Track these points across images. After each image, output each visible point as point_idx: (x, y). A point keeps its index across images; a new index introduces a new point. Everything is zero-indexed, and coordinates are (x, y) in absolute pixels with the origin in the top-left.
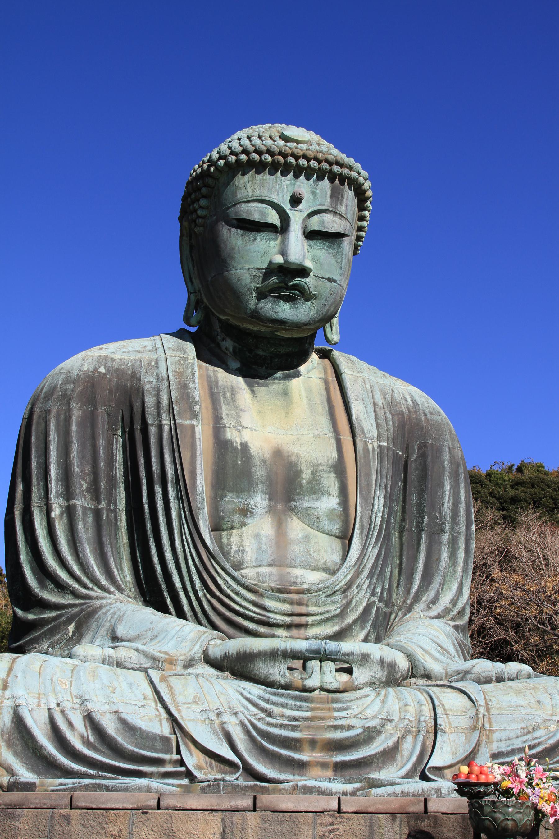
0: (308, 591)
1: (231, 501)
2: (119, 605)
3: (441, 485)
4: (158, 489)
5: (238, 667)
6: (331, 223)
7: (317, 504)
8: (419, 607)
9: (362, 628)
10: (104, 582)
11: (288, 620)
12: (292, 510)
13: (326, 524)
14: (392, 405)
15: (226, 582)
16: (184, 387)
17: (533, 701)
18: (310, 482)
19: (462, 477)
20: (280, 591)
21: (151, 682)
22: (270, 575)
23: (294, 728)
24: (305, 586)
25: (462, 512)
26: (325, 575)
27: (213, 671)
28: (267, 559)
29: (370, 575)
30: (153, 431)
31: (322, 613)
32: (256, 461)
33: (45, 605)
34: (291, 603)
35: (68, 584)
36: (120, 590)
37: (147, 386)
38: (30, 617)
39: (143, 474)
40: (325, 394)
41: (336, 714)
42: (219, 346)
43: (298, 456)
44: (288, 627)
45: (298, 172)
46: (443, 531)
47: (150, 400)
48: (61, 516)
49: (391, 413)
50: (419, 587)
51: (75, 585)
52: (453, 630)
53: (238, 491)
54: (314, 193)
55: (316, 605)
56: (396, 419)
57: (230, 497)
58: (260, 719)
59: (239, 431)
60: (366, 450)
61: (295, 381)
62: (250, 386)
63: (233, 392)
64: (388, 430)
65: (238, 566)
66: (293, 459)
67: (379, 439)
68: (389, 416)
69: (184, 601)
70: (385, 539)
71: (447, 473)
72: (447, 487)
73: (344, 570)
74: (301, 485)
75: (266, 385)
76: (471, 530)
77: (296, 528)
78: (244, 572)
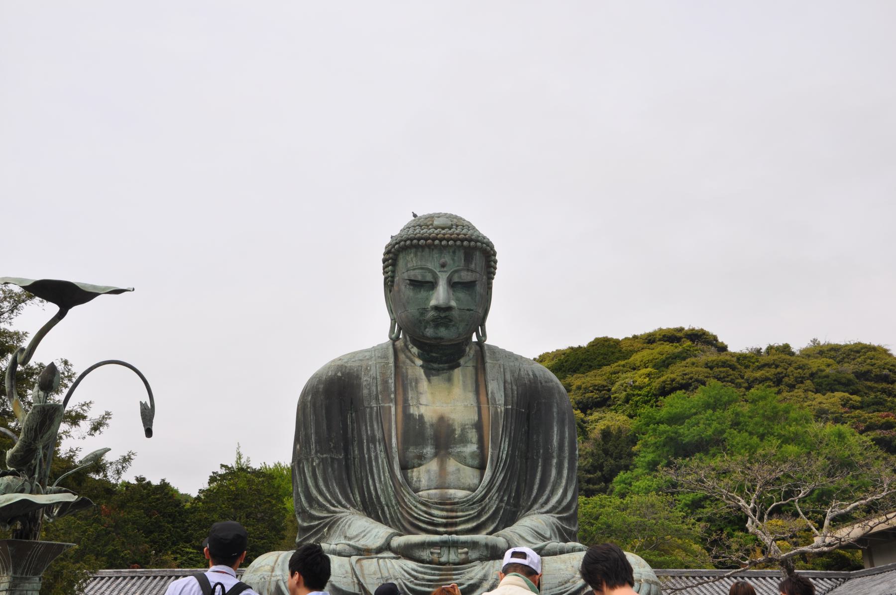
0: (457, 503)
1: (412, 451)
2: (350, 517)
3: (552, 428)
4: (371, 446)
5: (406, 552)
6: (466, 276)
7: (464, 449)
8: (536, 506)
9: (493, 523)
10: (344, 502)
11: (444, 521)
12: (450, 454)
13: (470, 461)
14: (518, 380)
15: (409, 500)
16: (385, 382)
17: (570, 566)
18: (460, 436)
19: (567, 421)
20: (440, 504)
21: (351, 564)
22: (436, 494)
23: (429, 586)
24: (456, 500)
25: (566, 444)
26: (468, 492)
27: (392, 555)
28: (434, 484)
29: (499, 490)
30: (368, 410)
31: (466, 516)
32: (428, 425)
33: (313, 518)
34: (447, 511)
35: (324, 506)
36: (354, 507)
37: (365, 383)
38: (305, 524)
39: (365, 437)
40: (474, 377)
41: (454, 577)
42: (410, 351)
43: (453, 420)
44: (445, 525)
45: (442, 249)
46: (553, 457)
47: (365, 391)
48: (318, 465)
49: (516, 385)
50: (537, 494)
51: (328, 505)
52: (555, 520)
53: (416, 444)
54: (453, 260)
55: (462, 511)
56: (520, 389)
57: (411, 449)
58: (411, 582)
59: (418, 407)
60: (496, 413)
61: (456, 370)
62: (428, 375)
63: (417, 381)
64: (513, 397)
65: (417, 490)
66: (451, 422)
67: (506, 404)
68: (515, 388)
69: (387, 512)
70: (510, 468)
71: (555, 420)
72: (555, 429)
73: (480, 488)
74: (455, 439)
75: (438, 375)
76: (575, 454)
77: (452, 465)
78: (420, 493)
